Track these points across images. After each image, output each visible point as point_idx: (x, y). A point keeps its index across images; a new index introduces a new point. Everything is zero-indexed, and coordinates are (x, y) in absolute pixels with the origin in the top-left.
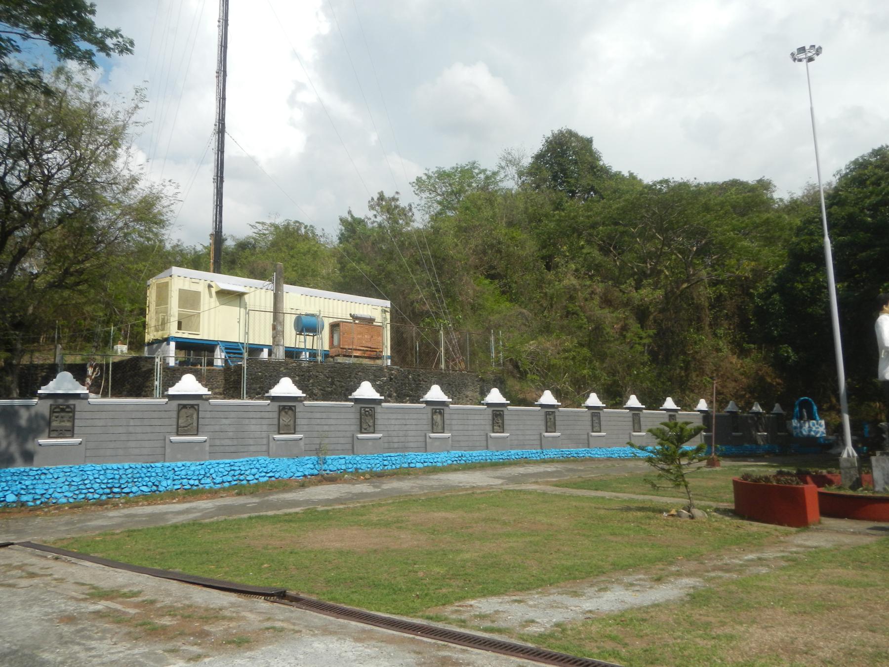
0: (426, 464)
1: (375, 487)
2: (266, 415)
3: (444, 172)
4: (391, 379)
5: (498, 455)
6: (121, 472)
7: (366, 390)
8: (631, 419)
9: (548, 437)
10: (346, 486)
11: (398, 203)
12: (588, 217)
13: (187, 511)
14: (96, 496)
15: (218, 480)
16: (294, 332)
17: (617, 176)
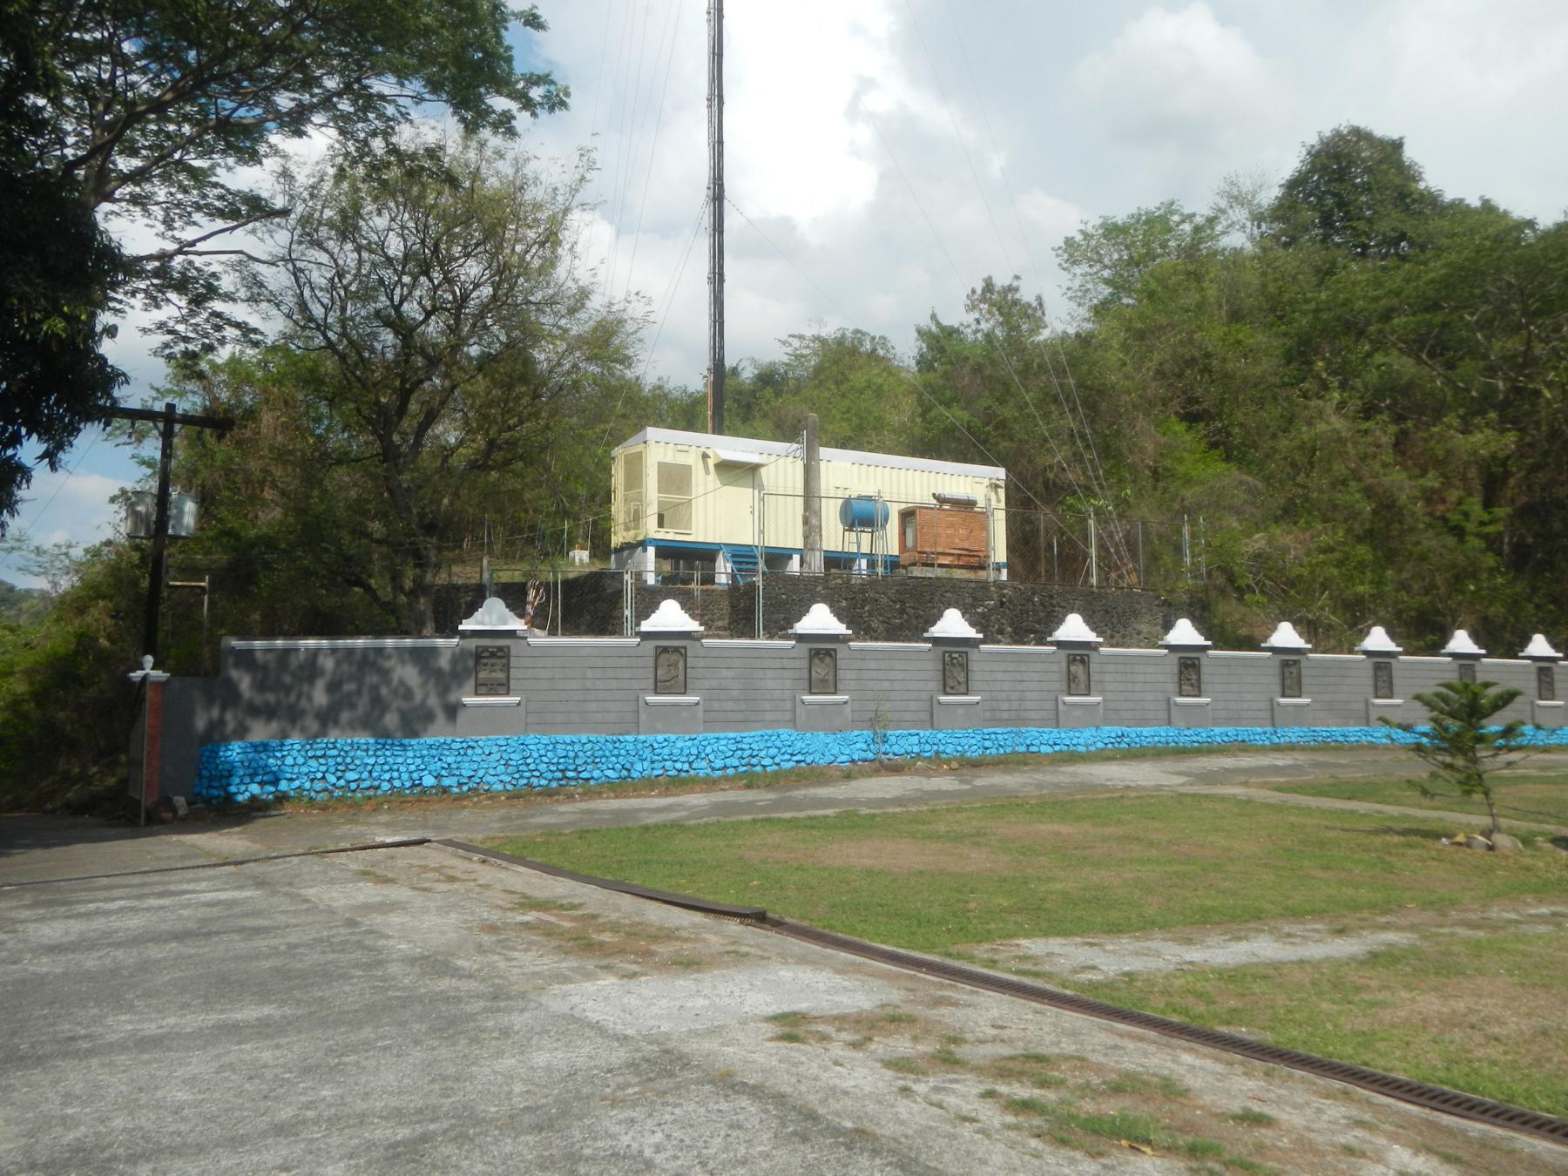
0: (1057, 748)
1: (962, 782)
2: (790, 664)
3: (1115, 225)
4: (1002, 604)
5: (1187, 736)
6: (577, 748)
7: (953, 624)
9: (1288, 705)
10: (917, 779)
11: (1017, 296)
12: (1376, 299)
13: (668, 809)
14: (544, 782)
15: (719, 764)
16: (841, 527)
17: (1458, 210)
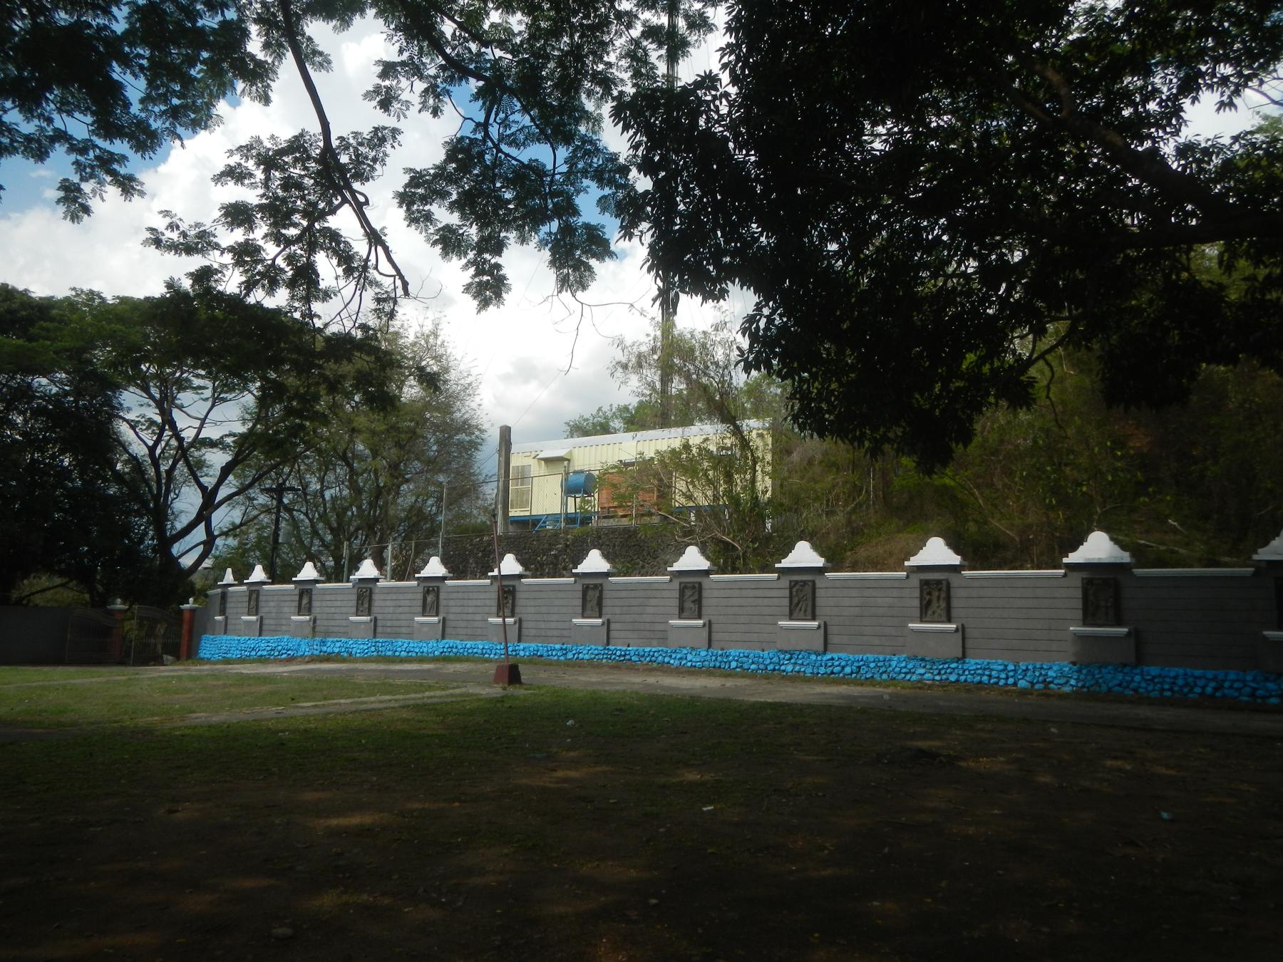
4: (567, 546)
8: (787, 593)
9: (581, 626)
